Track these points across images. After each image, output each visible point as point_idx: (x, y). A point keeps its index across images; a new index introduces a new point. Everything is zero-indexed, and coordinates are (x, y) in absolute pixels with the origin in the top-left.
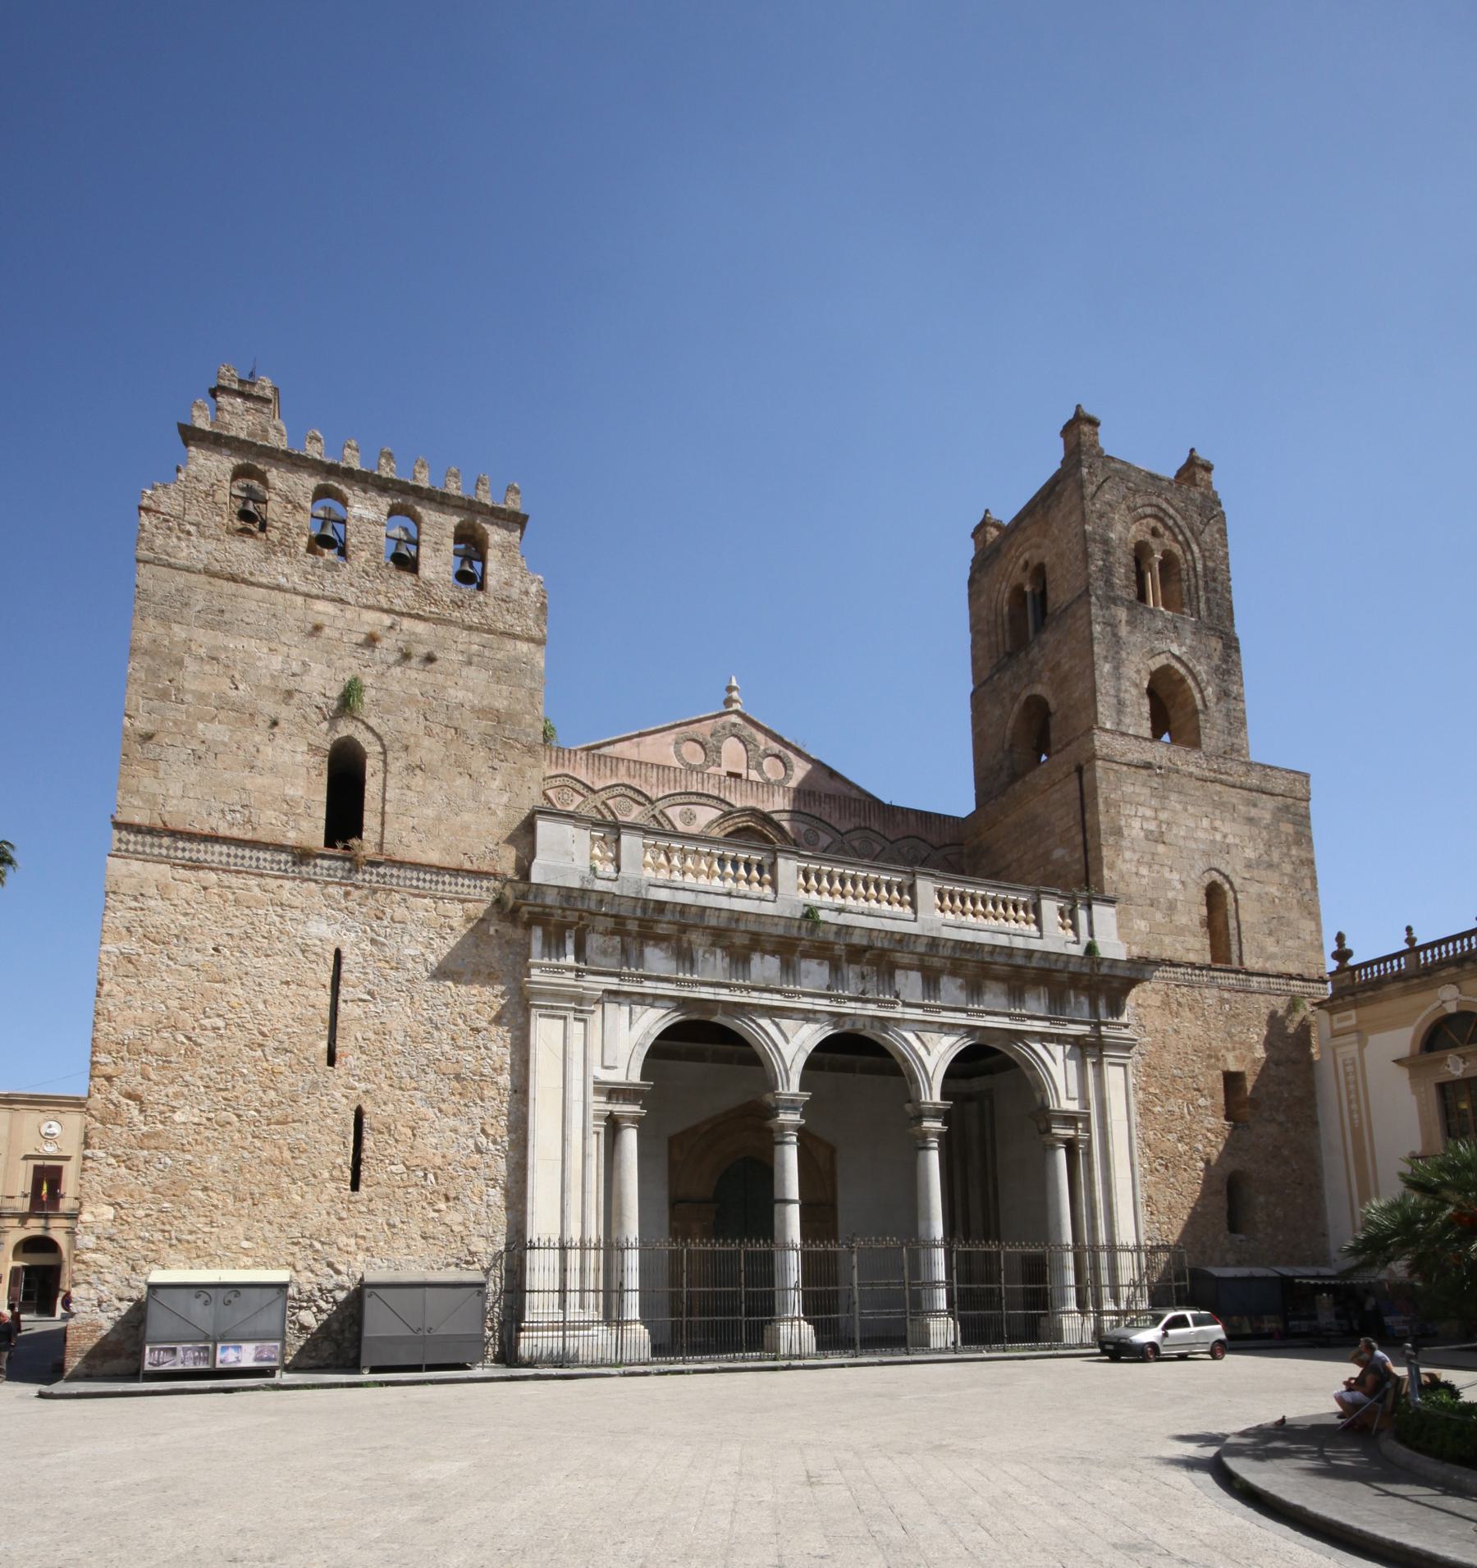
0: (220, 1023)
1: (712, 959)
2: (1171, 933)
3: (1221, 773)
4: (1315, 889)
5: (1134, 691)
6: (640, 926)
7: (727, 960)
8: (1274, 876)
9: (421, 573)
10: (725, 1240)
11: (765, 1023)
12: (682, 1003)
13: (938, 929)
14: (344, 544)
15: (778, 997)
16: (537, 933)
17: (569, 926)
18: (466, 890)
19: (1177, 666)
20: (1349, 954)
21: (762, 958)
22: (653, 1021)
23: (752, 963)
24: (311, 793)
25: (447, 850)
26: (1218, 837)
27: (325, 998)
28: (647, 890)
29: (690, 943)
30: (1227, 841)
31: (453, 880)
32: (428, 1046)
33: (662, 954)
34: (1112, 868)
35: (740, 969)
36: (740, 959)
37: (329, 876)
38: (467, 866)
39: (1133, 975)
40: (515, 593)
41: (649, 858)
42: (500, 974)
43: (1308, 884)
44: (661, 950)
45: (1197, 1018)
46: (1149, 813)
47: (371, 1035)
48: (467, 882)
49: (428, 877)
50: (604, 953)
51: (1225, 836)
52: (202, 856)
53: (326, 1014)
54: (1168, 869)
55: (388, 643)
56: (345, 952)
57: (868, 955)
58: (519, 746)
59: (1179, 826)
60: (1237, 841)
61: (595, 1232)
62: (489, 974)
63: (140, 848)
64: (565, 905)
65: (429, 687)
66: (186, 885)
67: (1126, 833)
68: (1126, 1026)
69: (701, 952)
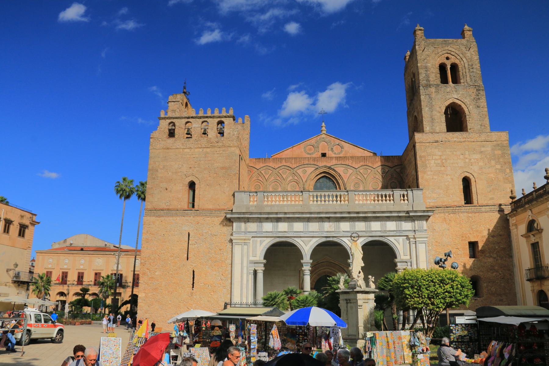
0: (164, 252)
18: (218, 214)
22: (267, 243)
26: (467, 160)
30: (471, 161)
37: (187, 215)
49: (209, 212)
58: (232, 175)
60: (475, 161)
67: (428, 166)
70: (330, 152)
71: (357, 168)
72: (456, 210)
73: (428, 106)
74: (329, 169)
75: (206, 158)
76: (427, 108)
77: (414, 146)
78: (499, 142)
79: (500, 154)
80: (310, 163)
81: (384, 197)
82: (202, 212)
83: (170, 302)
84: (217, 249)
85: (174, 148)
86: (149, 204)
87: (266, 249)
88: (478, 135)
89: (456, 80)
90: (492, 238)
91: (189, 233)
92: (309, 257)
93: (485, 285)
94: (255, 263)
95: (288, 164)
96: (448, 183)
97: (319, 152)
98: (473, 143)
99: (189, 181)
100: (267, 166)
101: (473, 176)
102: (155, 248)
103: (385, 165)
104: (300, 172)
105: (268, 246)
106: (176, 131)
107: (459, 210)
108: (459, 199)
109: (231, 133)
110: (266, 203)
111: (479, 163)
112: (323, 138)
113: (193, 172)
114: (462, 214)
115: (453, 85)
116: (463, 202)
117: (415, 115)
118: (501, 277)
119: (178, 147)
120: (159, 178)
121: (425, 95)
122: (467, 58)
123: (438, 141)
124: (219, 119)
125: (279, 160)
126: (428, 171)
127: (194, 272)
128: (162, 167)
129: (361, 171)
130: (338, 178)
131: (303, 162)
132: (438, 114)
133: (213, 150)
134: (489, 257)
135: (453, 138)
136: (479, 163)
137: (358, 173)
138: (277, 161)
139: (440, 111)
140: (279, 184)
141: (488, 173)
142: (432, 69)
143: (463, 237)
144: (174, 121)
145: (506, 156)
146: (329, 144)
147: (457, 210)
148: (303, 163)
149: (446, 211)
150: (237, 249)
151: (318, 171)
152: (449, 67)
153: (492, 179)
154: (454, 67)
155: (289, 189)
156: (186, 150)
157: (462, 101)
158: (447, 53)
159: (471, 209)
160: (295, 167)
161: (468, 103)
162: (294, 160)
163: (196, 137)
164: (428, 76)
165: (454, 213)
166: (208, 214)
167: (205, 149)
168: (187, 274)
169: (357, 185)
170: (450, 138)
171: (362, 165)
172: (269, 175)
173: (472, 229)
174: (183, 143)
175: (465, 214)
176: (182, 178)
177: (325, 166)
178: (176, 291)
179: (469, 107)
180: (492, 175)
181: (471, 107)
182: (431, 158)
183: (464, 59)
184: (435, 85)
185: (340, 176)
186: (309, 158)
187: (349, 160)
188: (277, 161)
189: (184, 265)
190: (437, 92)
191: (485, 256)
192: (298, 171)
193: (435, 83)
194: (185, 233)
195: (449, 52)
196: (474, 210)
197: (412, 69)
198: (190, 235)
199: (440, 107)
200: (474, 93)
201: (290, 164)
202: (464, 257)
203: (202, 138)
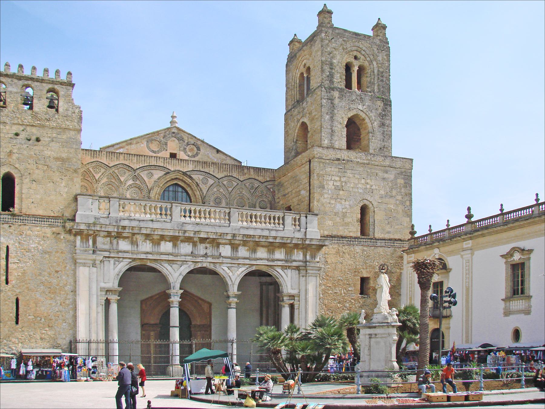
1: (145, 244)
2: (343, 226)
4: (411, 205)
5: (339, 126)
7: (151, 244)
8: (392, 201)
9: (34, 109)
10: (163, 340)
11: (166, 265)
12: (134, 260)
14: (5, 100)
15: (171, 257)
19: (361, 114)
20: (415, 233)
22: (123, 266)
29: (137, 239)
32: (40, 277)
36: (156, 243)
39: (321, 243)
40: (70, 113)
42: (65, 252)
43: (408, 203)
44: (125, 242)
45: (351, 258)
46: (337, 179)
47: (20, 274)
50: (104, 244)
54: (344, 200)
55: (23, 136)
56: (10, 246)
57: (208, 240)
61: (102, 337)
62: (62, 252)
64: (88, 229)
65: (37, 151)
68: (318, 262)
70: (182, 153)
71: (219, 178)
74: (183, 176)
81: (272, 219)
84: (52, 270)
95: (127, 163)
96: (346, 210)
97: (167, 150)
100: (98, 161)
101: (373, 205)
103: (254, 179)
104: (144, 175)
112: (174, 133)
116: (359, 234)
126: (326, 193)
127: (17, 300)
129: (225, 183)
131: (148, 161)
137: (221, 184)
140: (114, 189)
150: (83, 272)
151: (168, 177)
155: (128, 196)
160: (138, 167)
162: (136, 156)
169: (218, 199)
180: (392, 207)
185: (198, 185)
188: (113, 156)
192: (141, 174)
197: (305, 61)
198: (10, 250)
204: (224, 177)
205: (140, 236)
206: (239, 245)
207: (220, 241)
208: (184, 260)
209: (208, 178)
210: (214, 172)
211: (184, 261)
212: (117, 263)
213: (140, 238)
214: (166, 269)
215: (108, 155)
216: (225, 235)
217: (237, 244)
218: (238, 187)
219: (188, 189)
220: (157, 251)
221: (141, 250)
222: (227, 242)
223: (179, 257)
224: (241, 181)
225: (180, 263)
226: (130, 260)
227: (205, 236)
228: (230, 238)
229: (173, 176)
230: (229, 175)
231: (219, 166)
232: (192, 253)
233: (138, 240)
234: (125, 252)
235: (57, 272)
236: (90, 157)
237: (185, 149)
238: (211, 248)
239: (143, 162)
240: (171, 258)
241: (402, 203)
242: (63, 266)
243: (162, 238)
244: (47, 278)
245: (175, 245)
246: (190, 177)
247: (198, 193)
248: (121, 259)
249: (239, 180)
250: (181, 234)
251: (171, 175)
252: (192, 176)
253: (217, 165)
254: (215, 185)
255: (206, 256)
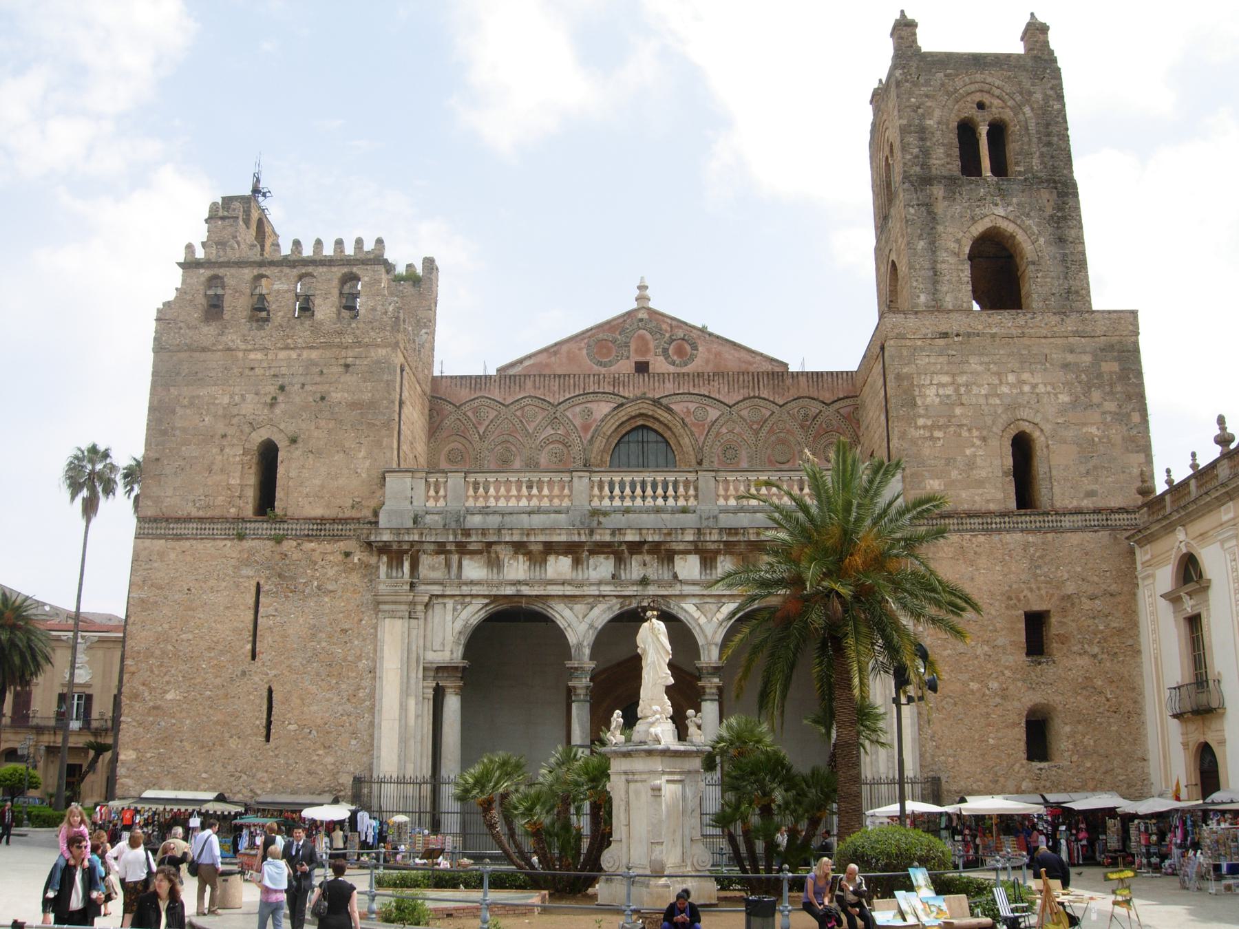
0: (191, 637)
1: (515, 564)
3: (1032, 328)
6: (456, 546)
8: (1097, 417)
12: (495, 598)
13: (716, 517)
15: (569, 588)
16: (385, 559)
17: (406, 552)
21: (557, 559)
22: (473, 614)
23: (548, 563)
24: (245, 482)
25: (328, 506)
26: (1026, 388)
27: (250, 615)
28: (465, 518)
30: (1037, 391)
31: (332, 527)
32: (313, 643)
33: (476, 565)
34: (903, 436)
35: (538, 569)
38: (341, 515)
41: (471, 492)
42: (361, 589)
48: (340, 527)
49: (315, 527)
50: (433, 568)
51: (1034, 386)
52: (183, 532)
53: (251, 627)
57: (646, 547)
58: (378, 423)
59: (980, 386)
63: (150, 531)
66: (174, 549)
67: (919, 402)
69: (506, 560)
72: (994, 526)
73: (925, 236)
75: (308, 377)
76: (922, 243)
77: (882, 348)
78: (1115, 339)
79: (1115, 373)
80: (601, 390)
82: (294, 527)
83: (204, 775)
85: (221, 347)
86: (150, 503)
87: (469, 630)
88: (1057, 318)
89: (1000, 168)
90: (1089, 602)
91: (258, 584)
92: (587, 651)
93: (1068, 729)
94: (438, 669)
96: (973, 449)
97: (628, 358)
98: (1043, 341)
99: (260, 440)
101: (1042, 430)
102: (166, 626)
103: (809, 398)
105: (475, 621)
106: (227, 303)
107: (1003, 525)
108: (1000, 495)
109: (379, 308)
110: (470, 503)
111: (1060, 396)
112: (641, 320)
113: (271, 416)
114: (1008, 536)
115: (996, 178)
116: (1012, 504)
117: (893, 261)
118: (1110, 707)
119: (230, 344)
120: (178, 432)
121: (918, 205)
122: (1035, 106)
123: (947, 333)
124: (345, 270)
125: (517, 382)
126: (920, 416)
128: (186, 402)
129: (744, 413)
130: (679, 429)
132: (952, 260)
133: (328, 354)
134: (1080, 654)
135: (990, 326)
136: (1060, 396)
138: (512, 384)
139: (957, 250)
141: (1085, 424)
142: (938, 134)
143: (1010, 598)
144: (221, 272)
145: (1131, 376)
146: (658, 336)
147: (996, 523)
148: (584, 389)
149: (965, 527)
151: (623, 413)
152: (983, 130)
153: (1093, 440)
154: (998, 132)
156: (252, 356)
157: (1019, 222)
158: (982, 91)
159: (1035, 522)
161: (1035, 229)
162: (557, 380)
163: (283, 317)
164: (926, 153)
165: (988, 531)
166: (310, 533)
167: (305, 354)
168: (252, 697)
170: (980, 327)
171: (747, 395)
172: (487, 423)
173: (1035, 576)
174: (244, 336)
175: (1018, 536)
176: (242, 431)
177: (643, 398)
178: (221, 745)
179: (1037, 240)
180: (1093, 430)
181: (1042, 240)
182: (928, 382)
183: (1027, 109)
184: (945, 177)
186: (599, 375)
187: (712, 383)
188: (512, 384)
189: (244, 673)
190: (950, 197)
191: (1068, 650)
192: (568, 414)
193: (945, 173)
194: (246, 584)
195: (987, 87)
196: (1042, 524)
199: (958, 241)
200: (1052, 203)
201: (547, 394)
202: (1012, 654)
203: (298, 322)
204: (741, 401)
205: (503, 546)
206: (718, 552)
207: (675, 547)
208: (597, 593)
209: (708, 408)
210: (719, 392)
211: (599, 596)
212: (459, 607)
213: (504, 553)
214: (563, 615)
215: (503, 382)
216: (680, 531)
217: (711, 551)
218: (773, 419)
219: (667, 434)
220: (538, 578)
221: (506, 578)
222: (691, 547)
223: (585, 588)
224: (781, 406)
225: (591, 600)
226: (487, 601)
227: (637, 538)
228: (691, 539)
229: (631, 410)
230: (752, 395)
231: (731, 379)
232: (614, 577)
233: (501, 557)
234: (472, 583)
235: (344, 631)
236: (468, 389)
237: (665, 351)
238: (655, 565)
239: (572, 388)
240: (569, 590)
241: (1121, 417)
242: (356, 619)
243: (550, 548)
244: (324, 644)
245: (577, 562)
246: (668, 409)
247: (687, 440)
248: (468, 600)
249: (774, 403)
250: (583, 538)
251: (629, 410)
252: (673, 407)
253: (726, 377)
254: (722, 421)
255: (644, 582)
